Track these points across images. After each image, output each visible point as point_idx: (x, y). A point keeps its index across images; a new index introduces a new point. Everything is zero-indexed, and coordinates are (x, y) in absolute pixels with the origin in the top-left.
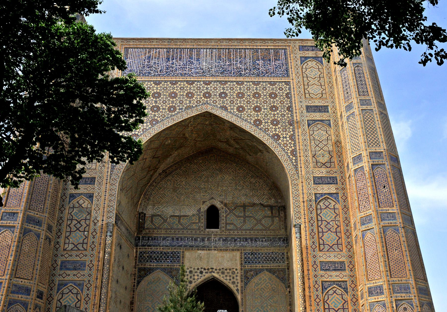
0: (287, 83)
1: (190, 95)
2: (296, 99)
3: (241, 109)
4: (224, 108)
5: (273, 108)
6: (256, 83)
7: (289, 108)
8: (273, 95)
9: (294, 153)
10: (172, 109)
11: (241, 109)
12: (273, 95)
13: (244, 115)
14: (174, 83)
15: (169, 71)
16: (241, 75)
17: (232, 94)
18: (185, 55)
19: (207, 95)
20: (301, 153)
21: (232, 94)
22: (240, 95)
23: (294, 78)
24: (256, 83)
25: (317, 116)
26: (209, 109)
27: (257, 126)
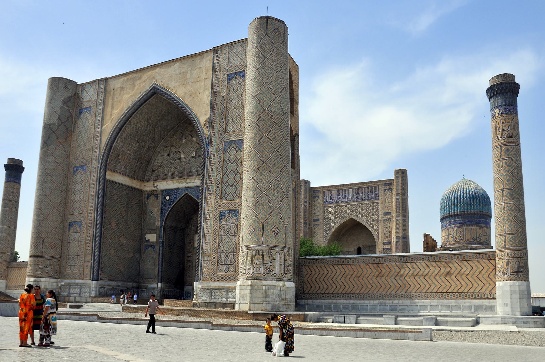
0: (378, 203)
1: (346, 211)
2: (381, 210)
3: (362, 216)
4: (357, 216)
5: (373, 215)
6: (367, 204)
7: (378, 214)
8: (373, 209)
9: (378, 233)
10: (340, 217)
11: (362, 216)
12: (373, 209)
13: (363, 218)
14: (341, 206)
15: (339, 201)
16: (362, 200)
17: (360, 210)
18: (344, 193)
19: (351, 211)
20: (380, 233)
21: (360, 210)
22: (362, 210)
23: (381, 201)
24: (367, 204)
25: (387, 217)
26: (352, 216)
27: (367, 222)
